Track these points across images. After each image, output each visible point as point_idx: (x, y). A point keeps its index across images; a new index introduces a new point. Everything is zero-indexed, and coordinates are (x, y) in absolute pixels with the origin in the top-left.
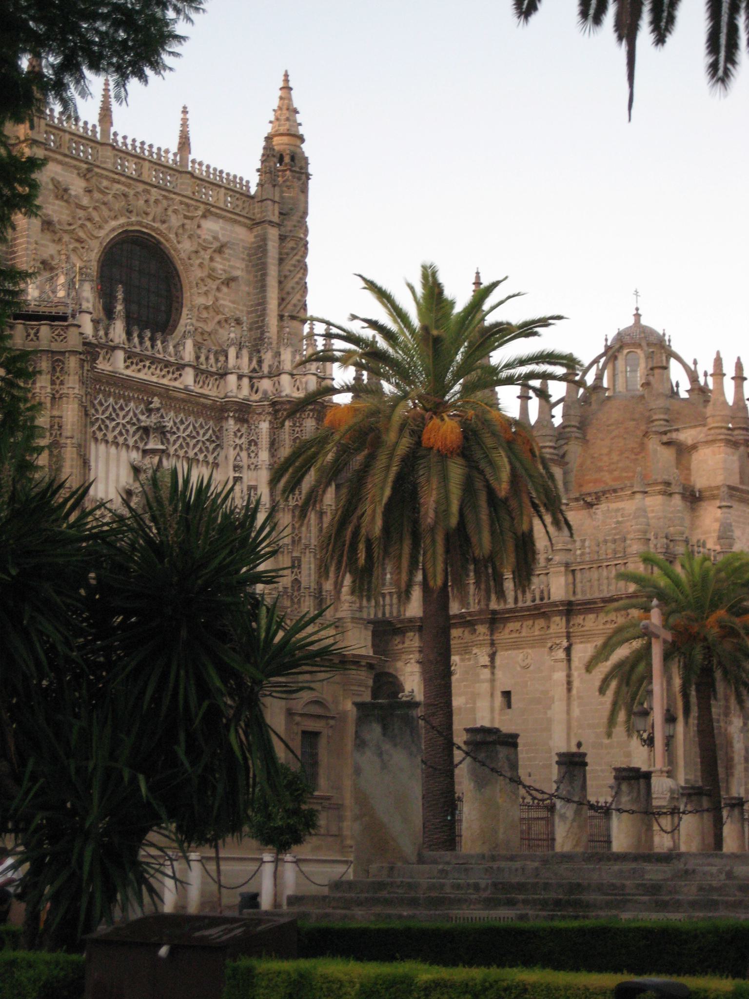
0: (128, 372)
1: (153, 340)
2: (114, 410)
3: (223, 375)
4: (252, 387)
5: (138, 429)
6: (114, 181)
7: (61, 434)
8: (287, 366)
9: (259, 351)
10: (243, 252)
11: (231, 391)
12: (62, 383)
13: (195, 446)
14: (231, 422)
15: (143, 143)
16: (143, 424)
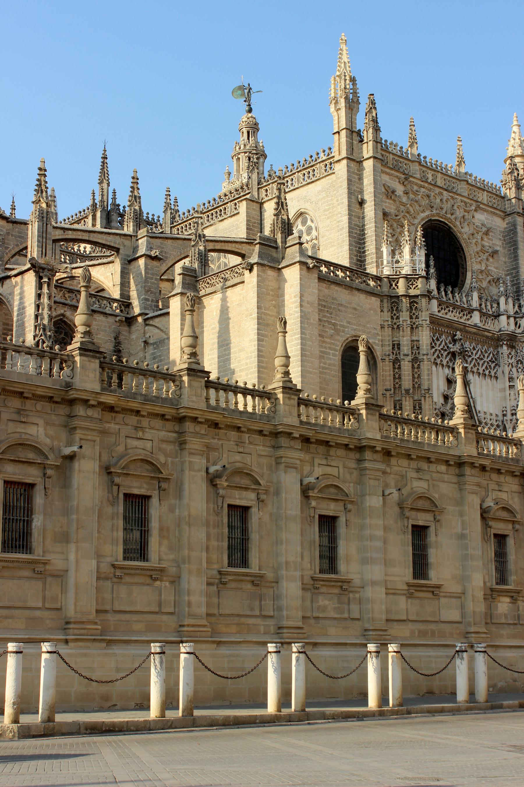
0: (440, 314)
3: (497, 316)
4: (516, 324)
5: (448, 354)
6: (421, 186)
7: (419, 353)
9: (518, 300)
10: (500, 235)
11: (504, 327)
12: (417, 317)
13: (483, 365)
14: (505, 347)
16: (451, 350)
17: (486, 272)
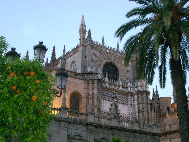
1: (114, 82)
2: (107, 94)
3: (127, 88)
5: (112, 97)
8: (140, 85)
12: (94, 86)
13: (123, 101)
14: (130, 96)
15: (110, 47)
17: (125, 76)
